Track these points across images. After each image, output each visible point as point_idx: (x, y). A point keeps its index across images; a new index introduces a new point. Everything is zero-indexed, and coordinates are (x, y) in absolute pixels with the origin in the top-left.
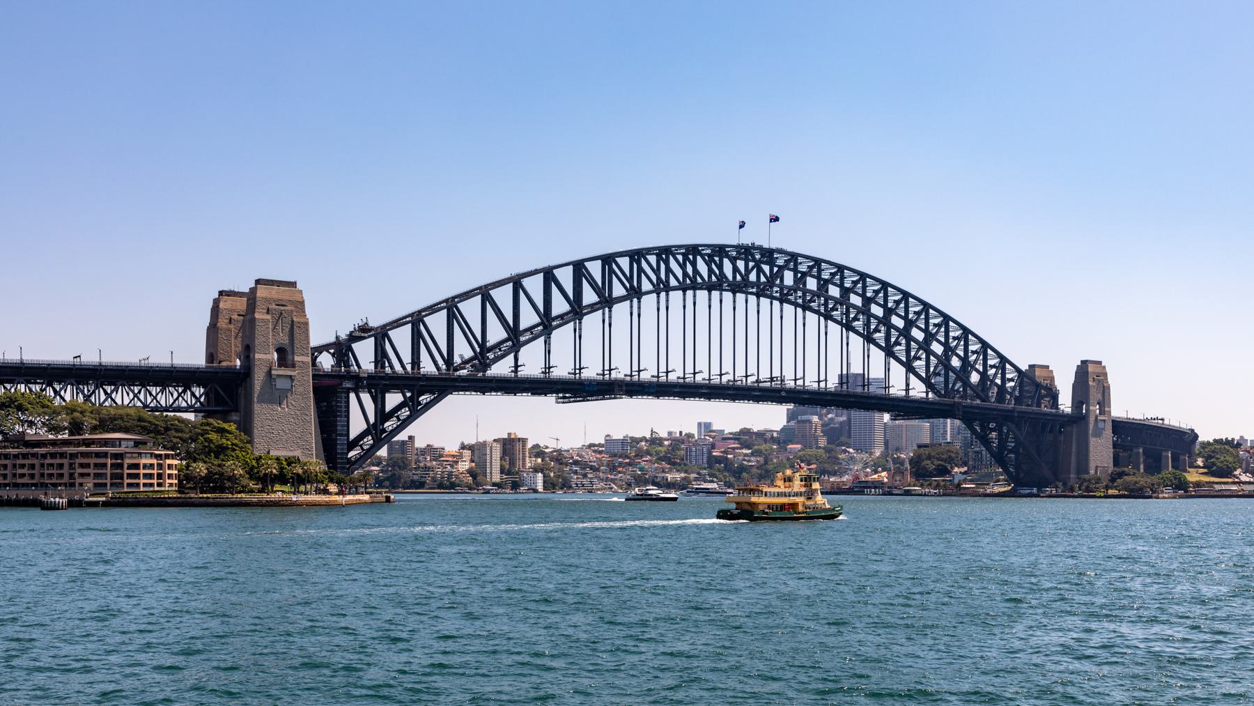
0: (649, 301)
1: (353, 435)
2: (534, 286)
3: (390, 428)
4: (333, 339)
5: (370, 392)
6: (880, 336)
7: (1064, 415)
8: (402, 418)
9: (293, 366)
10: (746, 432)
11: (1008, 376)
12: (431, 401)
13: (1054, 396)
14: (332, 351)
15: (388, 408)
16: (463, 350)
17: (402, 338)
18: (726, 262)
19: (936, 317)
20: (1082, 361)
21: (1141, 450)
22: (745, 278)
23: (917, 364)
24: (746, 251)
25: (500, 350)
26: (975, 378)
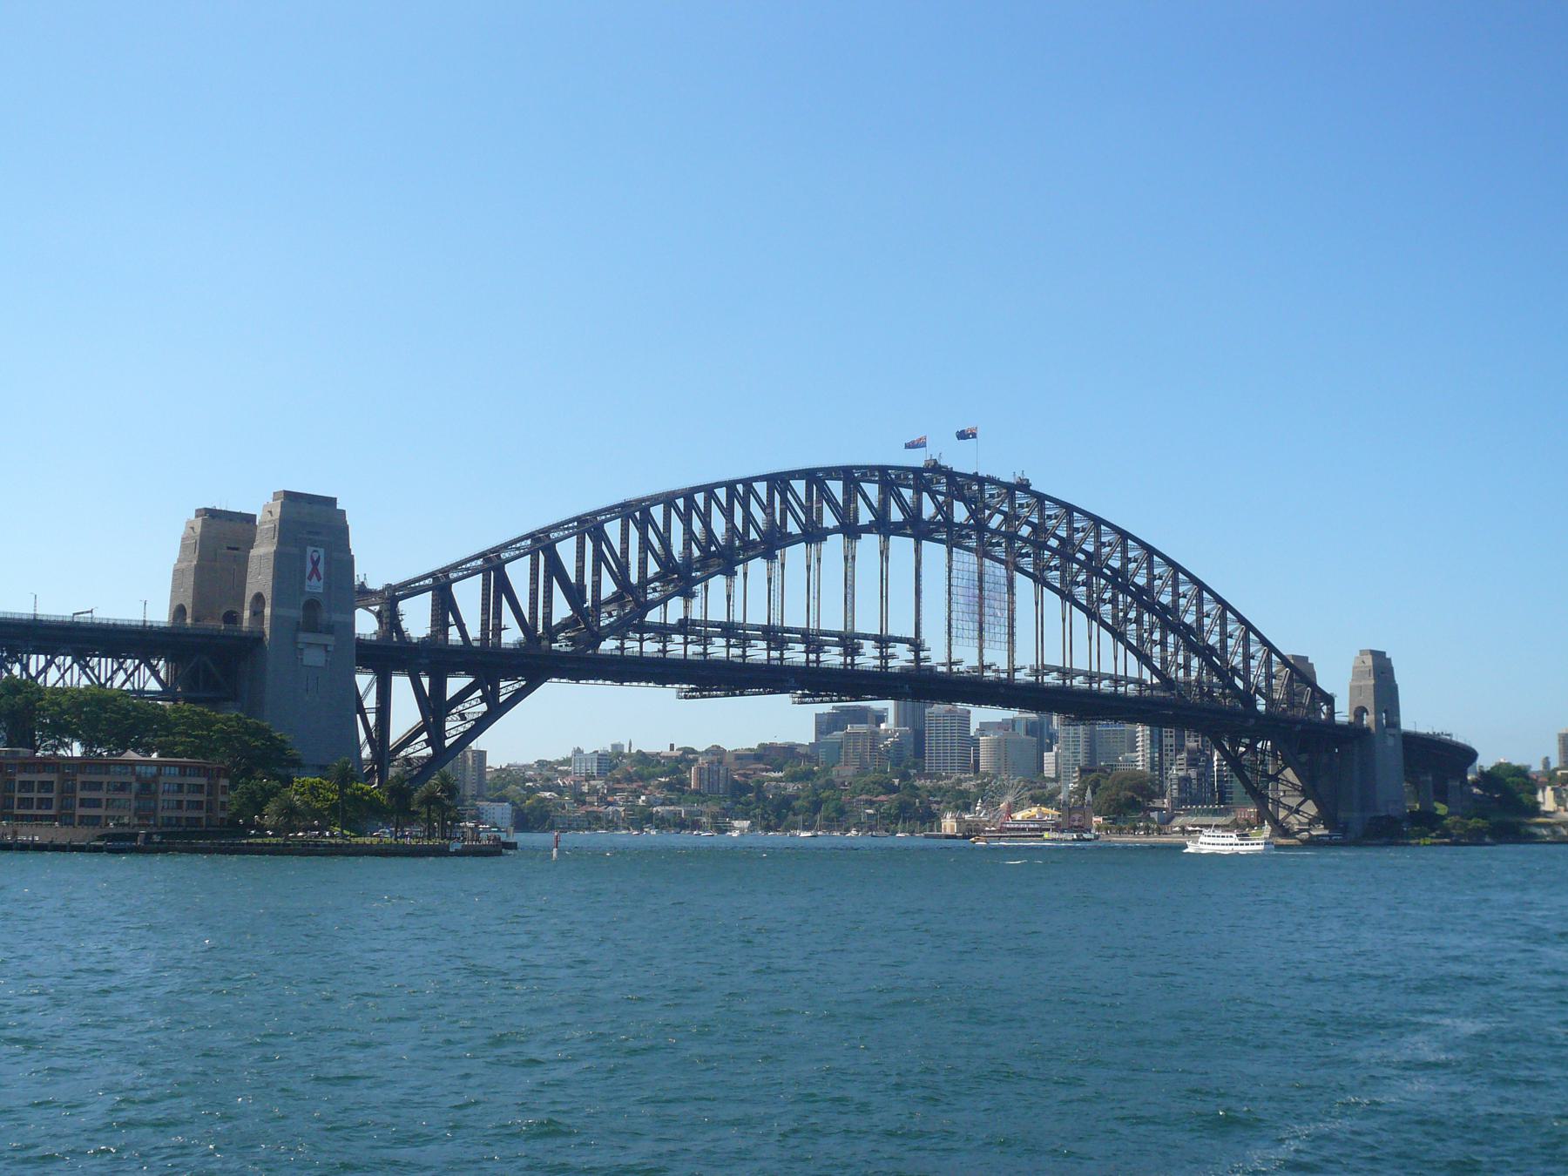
3: (453, 732)
6: (1106, 609)
7: (1342, 727)
9: (330, 629)
10: (763, 746)
13: (1329, 700)
17: (468, 595)
19: (1185, 583)
20: (1361, 651)
21: (1430, 778)
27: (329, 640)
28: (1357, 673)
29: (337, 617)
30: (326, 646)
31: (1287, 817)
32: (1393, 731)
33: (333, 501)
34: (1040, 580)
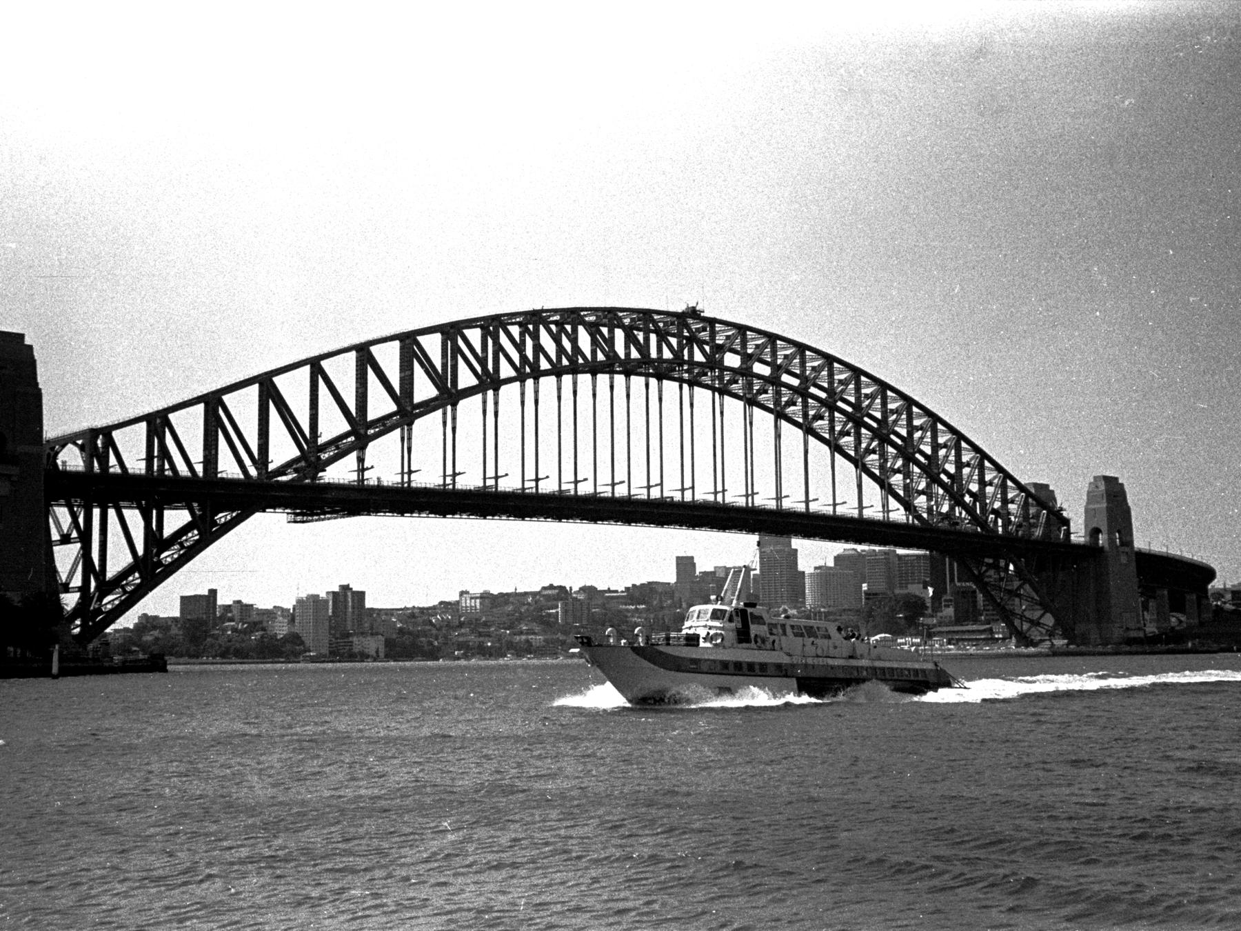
1: (111, 572)
2: (388, 357)
5: (139, 507)
7: (1078, 547)
8: (186, 544)
11: (1010, 496)
12: (233, 519)
13: (1066, 522)
14: (80, 442)
15: (168, 531)
16: (283, 450)
21: (1166, 592)
22: (677, 354)
25: (339, 448)
27: (14, 470)
28: (1091, 497)
29: (22, 449)
30: (9, 477)
31: (1029, 629)
32: (1127, 549)
33: (21, 337)
34: (780, 415)
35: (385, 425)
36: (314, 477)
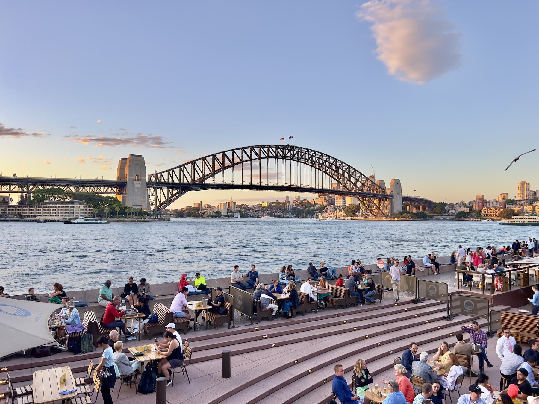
0: (255, 163)
4: (154, 173)
9: (141, 180)
15: (174, 193)
18: (279, 150)
23: (340, 180)
24: (285, 147)
25: (209, 176)
26: (359, 184)
27: (140, 182)
29: (142, 178)
35: (219, 171)
36: (202, 183)
